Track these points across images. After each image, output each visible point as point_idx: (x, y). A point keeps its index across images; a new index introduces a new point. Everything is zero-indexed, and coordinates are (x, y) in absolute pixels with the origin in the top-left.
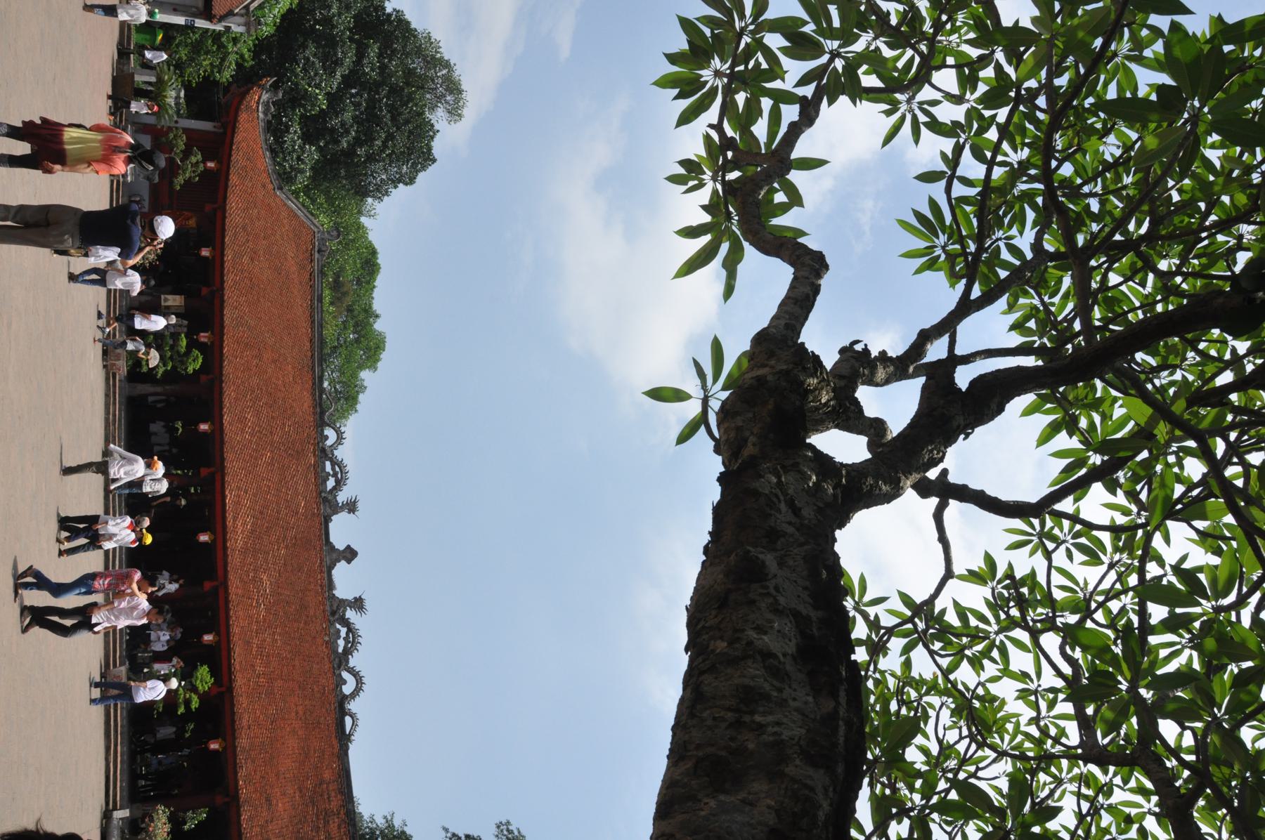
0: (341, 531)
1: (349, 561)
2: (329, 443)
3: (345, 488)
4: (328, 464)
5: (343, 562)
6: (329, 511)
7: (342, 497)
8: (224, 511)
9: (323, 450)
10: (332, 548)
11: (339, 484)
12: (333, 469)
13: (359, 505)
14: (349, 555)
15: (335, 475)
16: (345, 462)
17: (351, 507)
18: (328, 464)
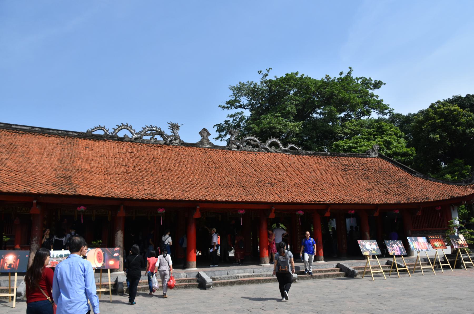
0: (189, 135)
1: (209, 134)
2: (130, 136)
3: (162, 129)
4: (144, 138)
5: (209, 138)
6: (177, 141)
7: (168, 132)
8: (232, 202)
9: (136, 139)
10: (201, 143)
11: (161, 134)
12: (149, 135)
13: (174, 122)
14: (205, 134)
15: (153, 135)
16: (144, 127)
17: (174, 127)
18: (144, 138)
